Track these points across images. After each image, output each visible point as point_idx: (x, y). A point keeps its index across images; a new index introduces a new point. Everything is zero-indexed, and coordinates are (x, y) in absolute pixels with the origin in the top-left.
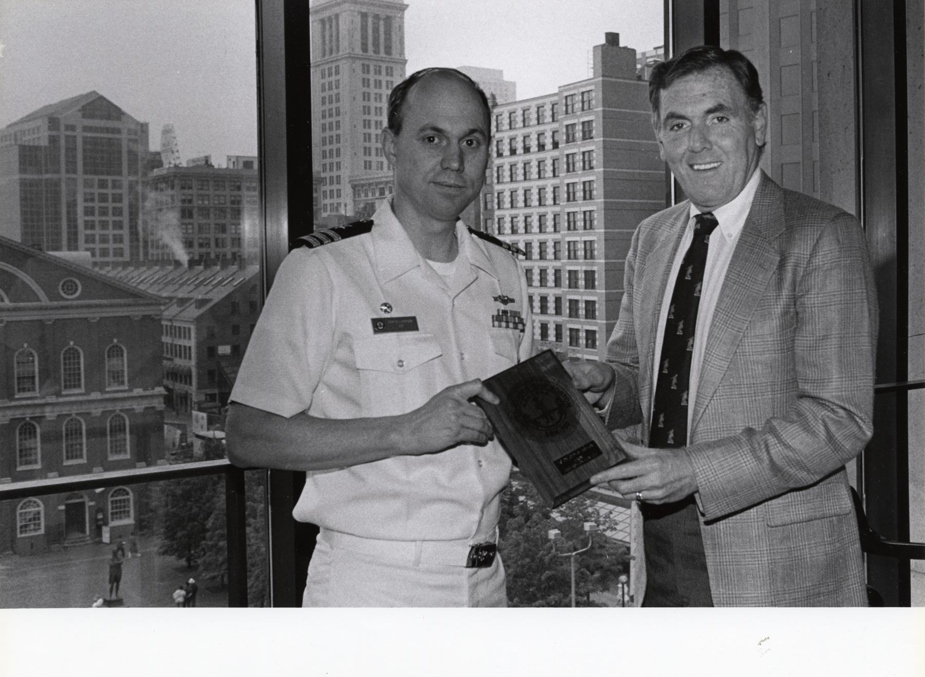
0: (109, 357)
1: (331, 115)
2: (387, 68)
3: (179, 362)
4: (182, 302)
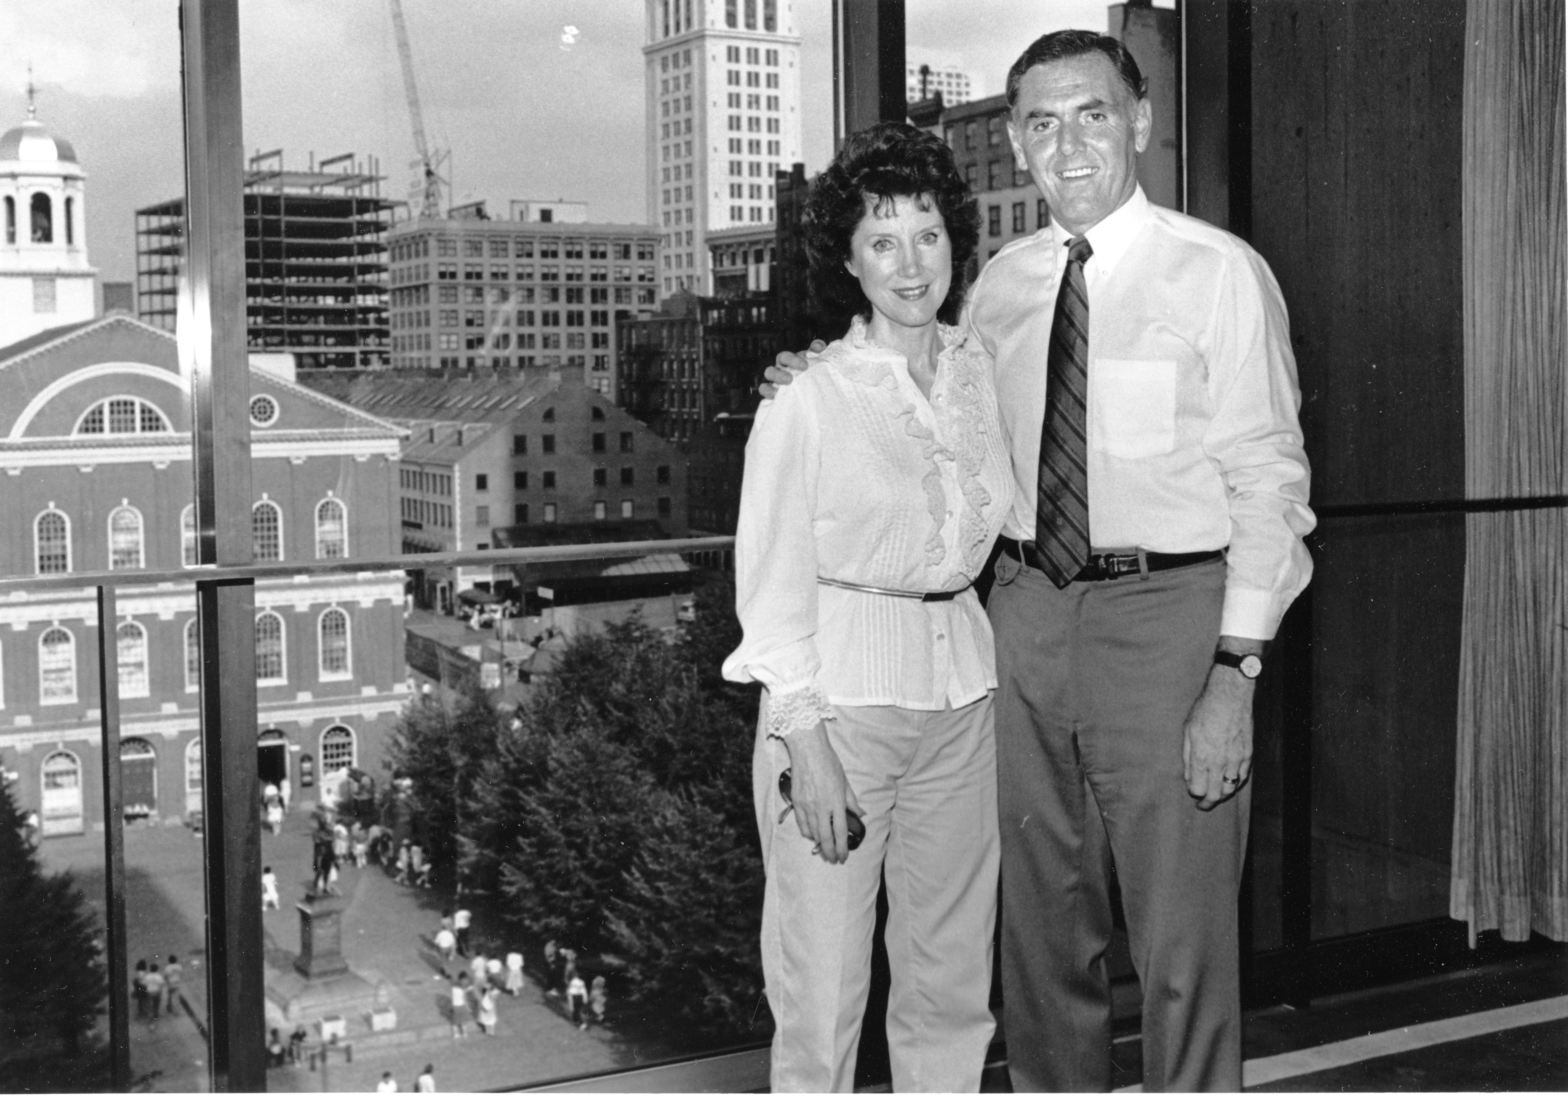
0: (321, 517)
1: (678, 133)
2: (768, 52)
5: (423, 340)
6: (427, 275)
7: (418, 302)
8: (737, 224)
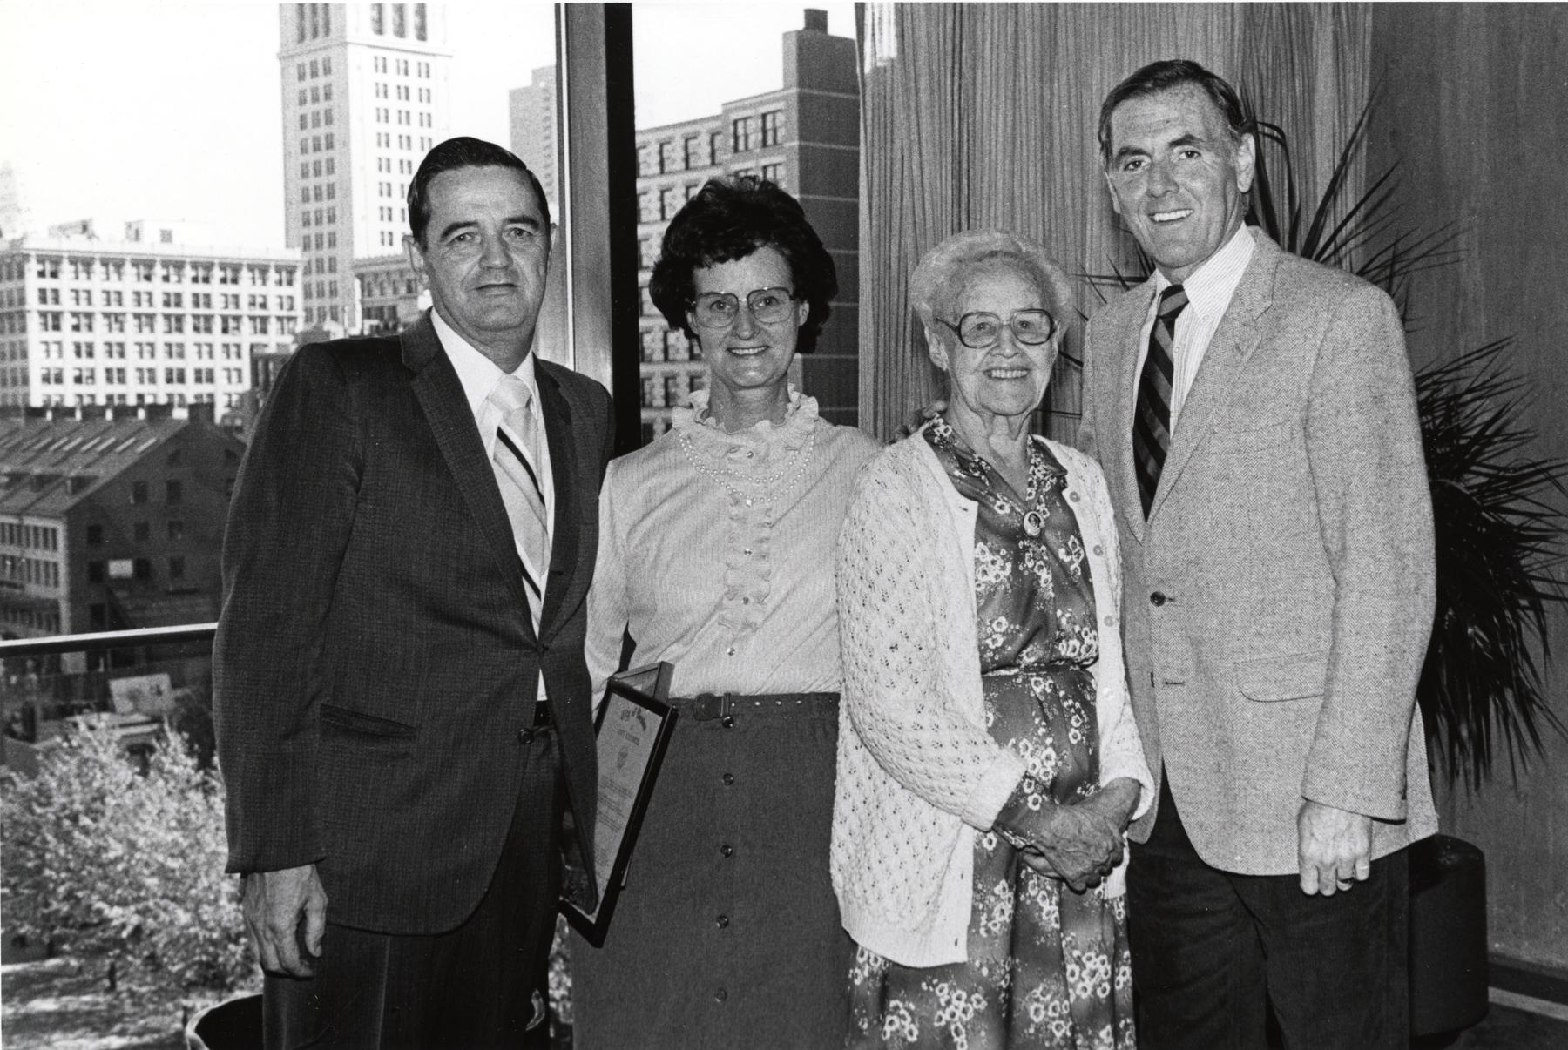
1: (317, 148)
3: (35, 590)
4: (42, 482)
5: (19, 375)
6: (22, 301)
7: (12, 330)
8: (387, 251)
